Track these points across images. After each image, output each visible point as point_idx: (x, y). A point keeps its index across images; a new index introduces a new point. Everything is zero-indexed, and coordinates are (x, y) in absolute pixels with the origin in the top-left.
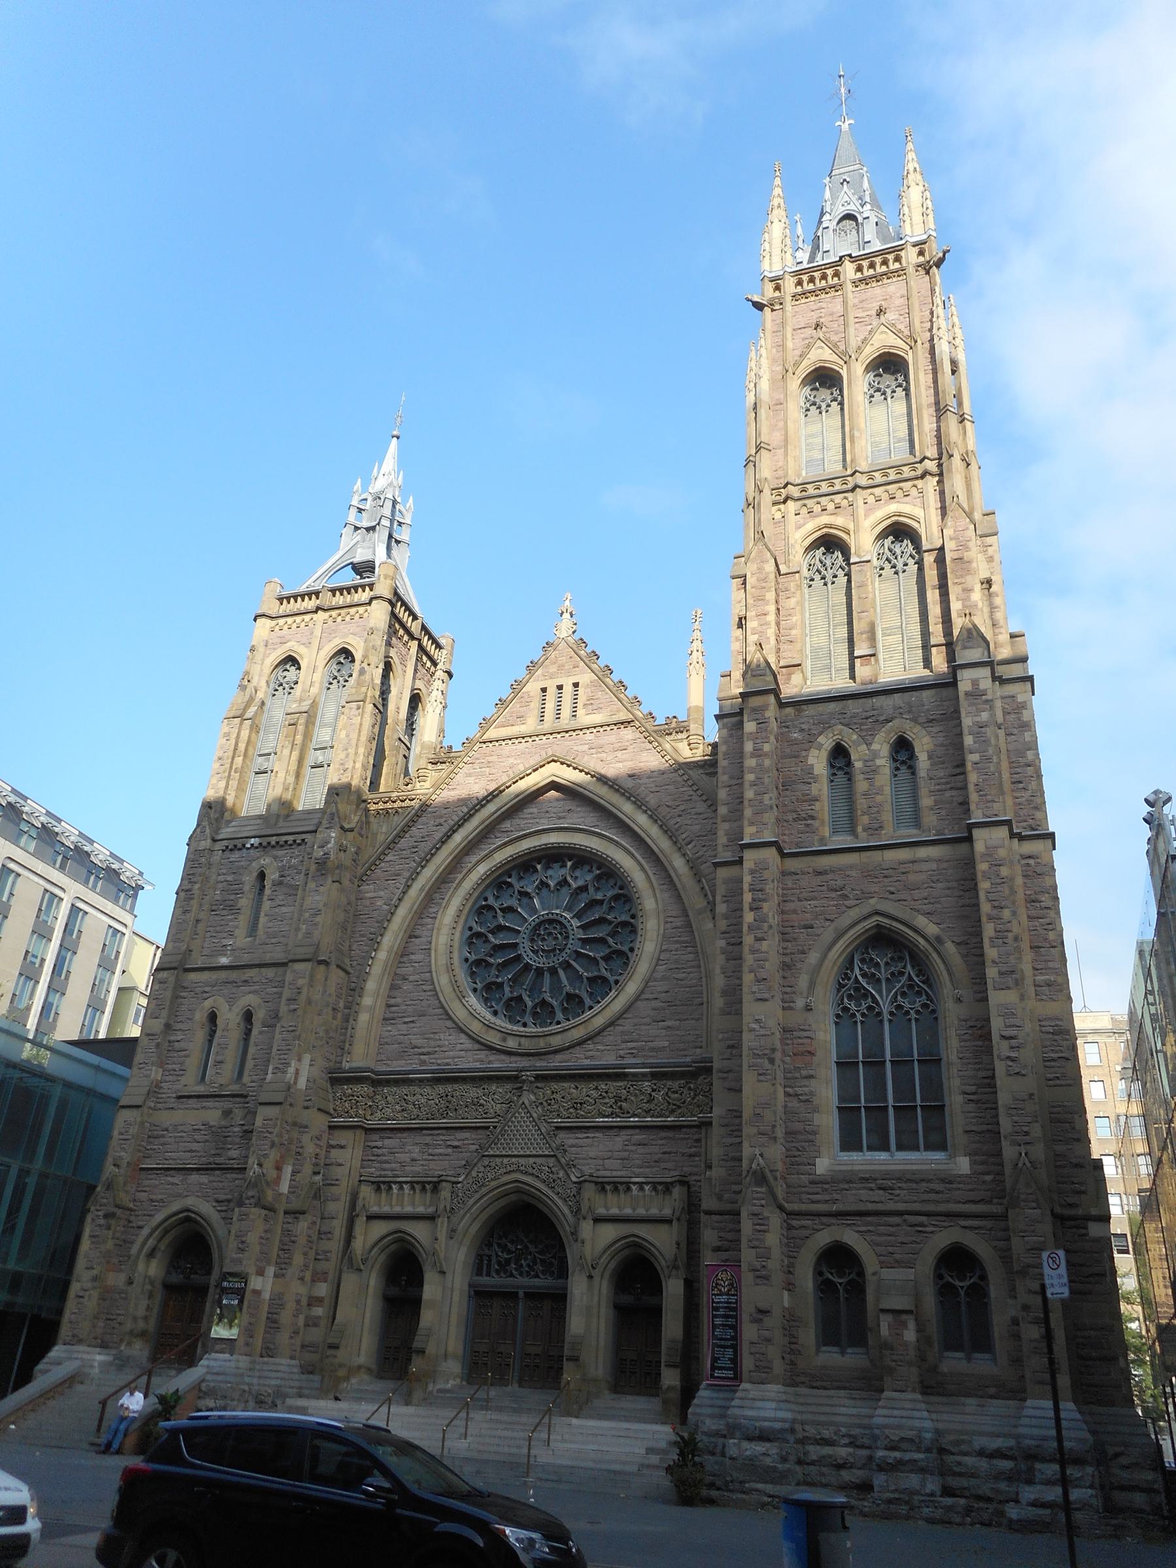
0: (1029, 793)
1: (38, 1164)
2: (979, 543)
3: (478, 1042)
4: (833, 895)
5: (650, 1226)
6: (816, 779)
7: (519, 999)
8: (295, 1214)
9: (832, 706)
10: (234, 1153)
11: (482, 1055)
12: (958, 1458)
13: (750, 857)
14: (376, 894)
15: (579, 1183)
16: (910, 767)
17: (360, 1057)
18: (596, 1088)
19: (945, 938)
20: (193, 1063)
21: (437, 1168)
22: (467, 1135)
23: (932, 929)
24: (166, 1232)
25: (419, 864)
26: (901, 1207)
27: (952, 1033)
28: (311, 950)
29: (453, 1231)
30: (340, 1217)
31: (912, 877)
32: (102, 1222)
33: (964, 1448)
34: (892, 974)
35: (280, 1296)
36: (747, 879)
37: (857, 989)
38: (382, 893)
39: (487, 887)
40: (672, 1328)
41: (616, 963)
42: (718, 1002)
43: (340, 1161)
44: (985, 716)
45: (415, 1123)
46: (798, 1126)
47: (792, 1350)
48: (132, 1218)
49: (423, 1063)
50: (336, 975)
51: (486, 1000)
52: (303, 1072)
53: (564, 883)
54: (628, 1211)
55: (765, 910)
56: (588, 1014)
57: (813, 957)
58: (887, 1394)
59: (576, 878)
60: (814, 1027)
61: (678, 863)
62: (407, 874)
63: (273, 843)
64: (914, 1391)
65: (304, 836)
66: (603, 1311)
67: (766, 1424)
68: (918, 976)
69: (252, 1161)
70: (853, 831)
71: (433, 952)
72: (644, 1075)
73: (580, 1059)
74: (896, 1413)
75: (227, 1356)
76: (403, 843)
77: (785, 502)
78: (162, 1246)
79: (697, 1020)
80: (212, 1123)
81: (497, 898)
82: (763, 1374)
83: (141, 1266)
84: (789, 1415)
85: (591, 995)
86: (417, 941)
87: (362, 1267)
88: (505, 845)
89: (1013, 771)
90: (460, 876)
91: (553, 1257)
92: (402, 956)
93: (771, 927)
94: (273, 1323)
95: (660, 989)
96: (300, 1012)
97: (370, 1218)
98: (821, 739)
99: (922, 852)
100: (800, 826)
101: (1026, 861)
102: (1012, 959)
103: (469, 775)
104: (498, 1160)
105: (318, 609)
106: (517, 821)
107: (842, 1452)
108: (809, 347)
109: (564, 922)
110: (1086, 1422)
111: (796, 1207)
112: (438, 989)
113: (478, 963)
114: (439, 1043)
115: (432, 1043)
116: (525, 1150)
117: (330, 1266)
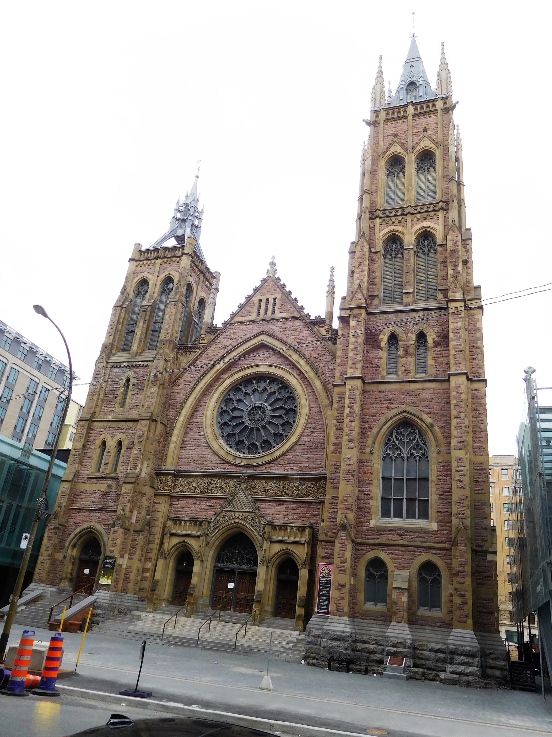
0: (477, 361)
1: (25, 503)
2: (463, 243)
3: (223, 460)
4: (386, 402)
5: (295, 546)
6: (381, 349)
7: (242, 441)
8: (138, 532)
9: (391, 316)
10: (112, 504)
11: (225, 466)
12: (421, 652)
13: (349, 383)
14: (180, 391)
16: (425, 346)
17: (169, 464)
18: (275, 483)
19: (434, 424)
20: (94, 463)
21: (202, 515)
22: (216, 501)
23: (429, 420)
24: (81, 537)
25: (200, 378)
26: (406, 543)
27: (434, 467)
28: (149, 415)
29: (209, 543)
30: (158, 533)
31: (422, 396)
32: (53, 531)
33: (424, 648)
34: (410, 440)
35: (130, 567)
36: (348, 393)
37: (393, 445)
38: (182, 390)
39: (230, 390)
40: (302, 591)
41: (287, 428)
42: (331, 448)
43: (159, 510)
44: (460, 324)
45: (193, 495)
46: (363, 505)
47: (353, 603)
48: (66, 530)
49: (198, 468)
50: (160, 427)
51: (227, 441)
52: (145, 470)
53: (265, 390)
54: (286, 538)
55: (355, 408)
56: (273, 450)
57: (375, 430)
58: (393, 623)
59: (271, 387)
60: (374, 461)
61: (318, 384)
62: (194, 382)
63: (134, 365)
64: (405, 622)
66: (272, 581)
67: (340, 633)
68: (421, 441)
70: (396, 374)
71: (204, 418)
72: (296, 478)
73: (268, 470)
74: (396, 631)
75: (106, 592)
76: (193, 368)
77: (375, 219)
78: (79, 543)
79: (322, 455)
80: (102, 490)
81: (234, 395)
82: (340, 612)
83: (70, 551)
84: (349, 630)
85: (275, 441)
86: (198, 413)
87: (167, 557)
88: (239, 371)
89: (471, 350)
90: (218, 384)
91: (252, 557)
92: (190, 419)
93: (357, 415)
94: (127, 578)
95: (306, 440)
96: (143, 443)
97: (172, 535)
98: (385, 330)
99: (427, 385)
100: (373, 370)
101: (473, 392)
102: (464, 436)
103: (225, 338)
105: (158, 257)
106: (246, 360)
107: (372, 647)
108: (390, 145)
109: (265, 407)
110: (477, 639)
111: (360, 541)
112: (206, 435)
113: (224, 424)
114: (205, 459)
115: (202, 459)
116: (241, 510)
117: (153, 555)
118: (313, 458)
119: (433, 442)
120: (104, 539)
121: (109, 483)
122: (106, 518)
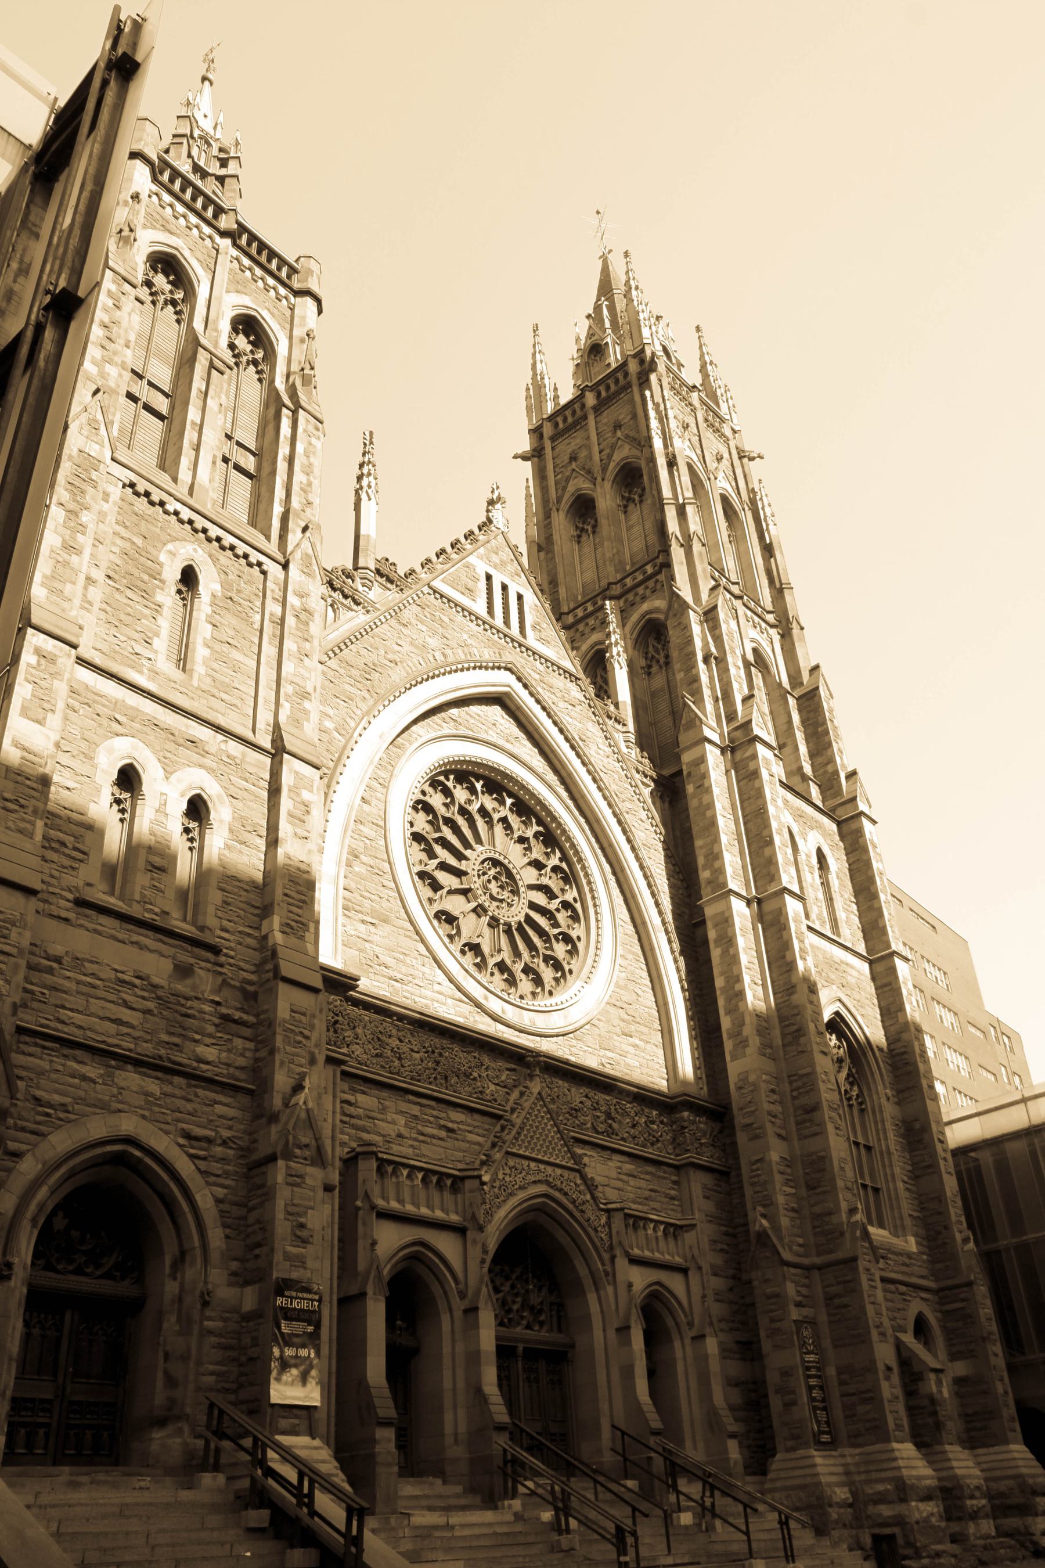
3: (459, 989)
15: (608, 1211)
27: (889, 1126)
65: (263, 558)
69: (282, 1080)
80: (156, 980)
104: (525, 1163)
115: (404, 969)
120: (198, 1197)
121: (185, 958)
122: (189, 1107)
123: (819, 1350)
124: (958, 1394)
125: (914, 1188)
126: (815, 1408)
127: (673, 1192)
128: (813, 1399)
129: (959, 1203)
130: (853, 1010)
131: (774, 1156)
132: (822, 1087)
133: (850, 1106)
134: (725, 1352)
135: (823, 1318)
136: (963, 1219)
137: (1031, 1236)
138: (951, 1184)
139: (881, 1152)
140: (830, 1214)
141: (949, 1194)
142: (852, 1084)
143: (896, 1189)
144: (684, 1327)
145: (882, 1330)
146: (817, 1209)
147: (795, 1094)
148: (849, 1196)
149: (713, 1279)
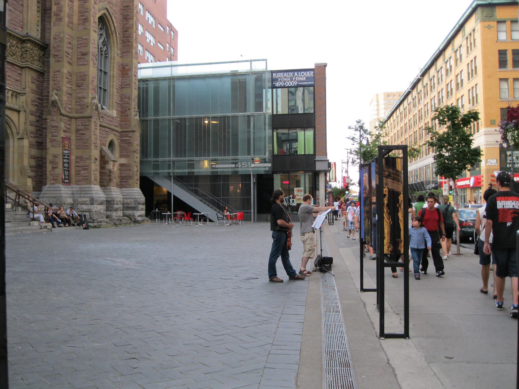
26: (105, 125)
27: (116, 66)
118: (13, 13)
119: (115, 44)
123: (70, 149)
124: (120, 170)
125: (120, 92)
126: (64, 170)
127: (18, 78)
128: (64, 167)
129: (137, 101)
130: (111, 14)
131: (65, 71)
132: (91, 45)
133: (101, 54)
134: (31, 146)
135: (73, 137)
136: (137, 107)
137: (160, 117)
138: (135, 93)
139: (110, 76)
140: (84, 98)
141: (133, 97)
142: (104, 45)
143: (113, 91)
144: (15, 134)
145: (96, 145)
146: (79, 95)
147: (79, 46)
148: (93, 92)
149: (30, 116)
